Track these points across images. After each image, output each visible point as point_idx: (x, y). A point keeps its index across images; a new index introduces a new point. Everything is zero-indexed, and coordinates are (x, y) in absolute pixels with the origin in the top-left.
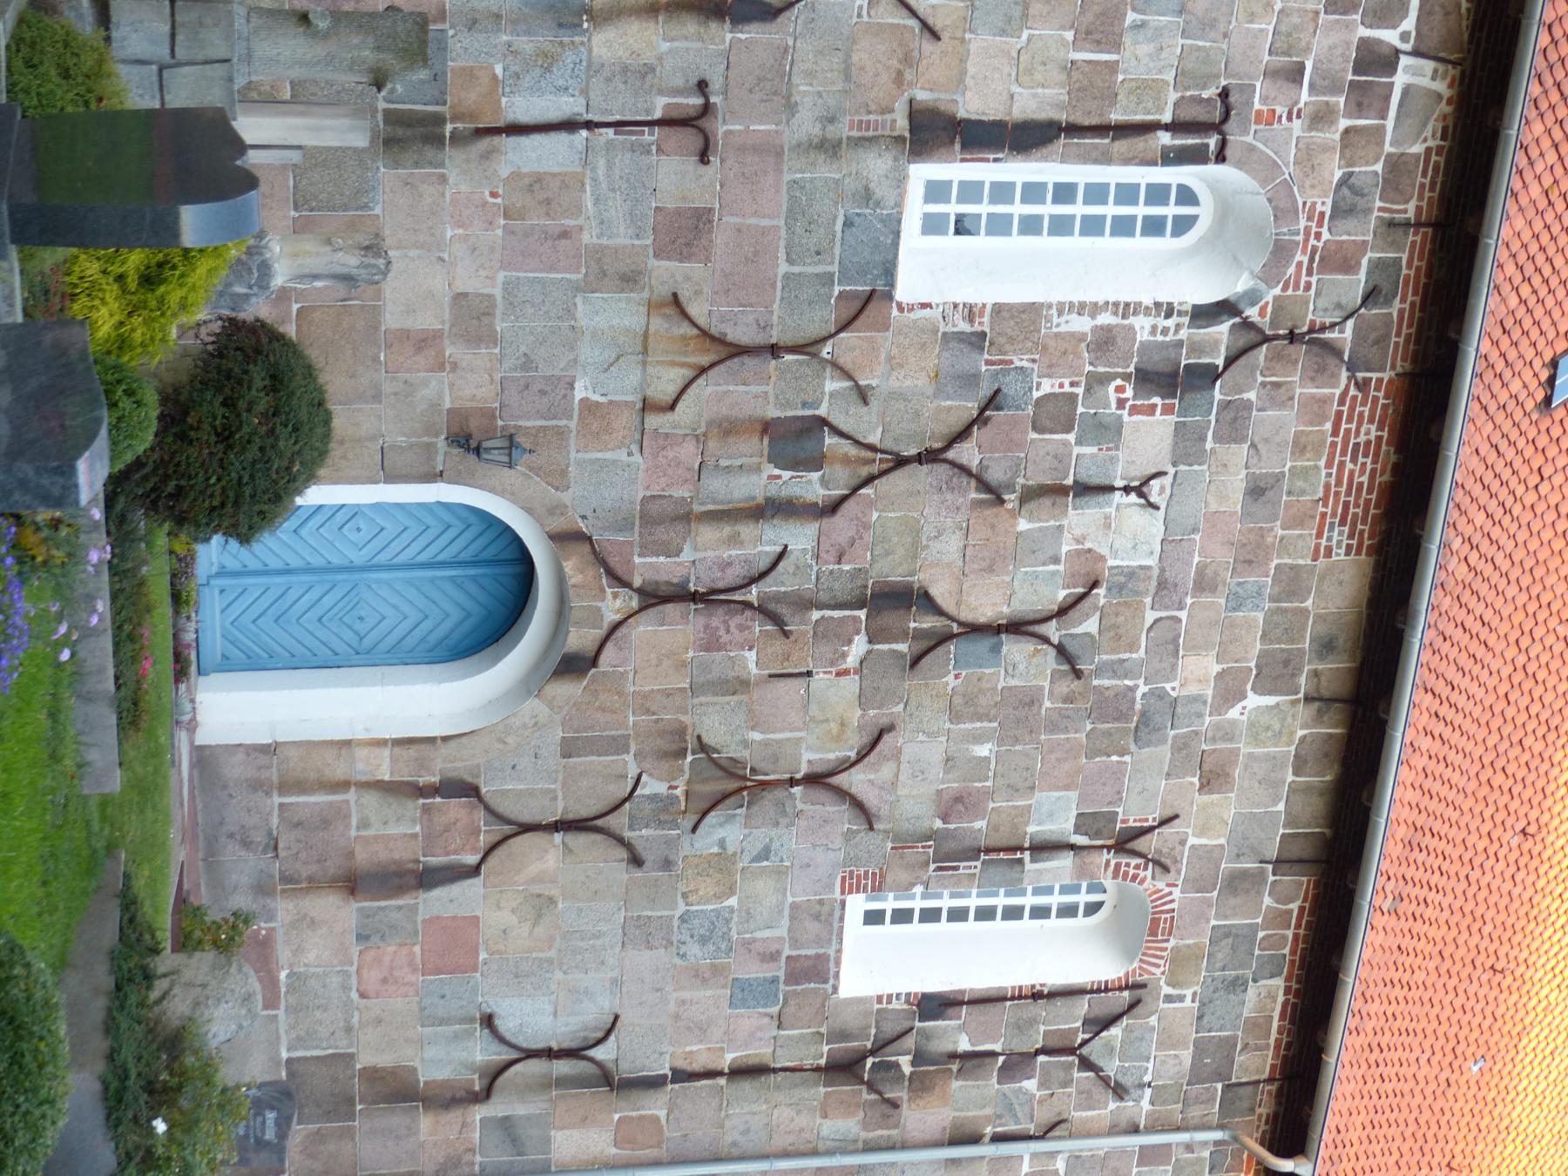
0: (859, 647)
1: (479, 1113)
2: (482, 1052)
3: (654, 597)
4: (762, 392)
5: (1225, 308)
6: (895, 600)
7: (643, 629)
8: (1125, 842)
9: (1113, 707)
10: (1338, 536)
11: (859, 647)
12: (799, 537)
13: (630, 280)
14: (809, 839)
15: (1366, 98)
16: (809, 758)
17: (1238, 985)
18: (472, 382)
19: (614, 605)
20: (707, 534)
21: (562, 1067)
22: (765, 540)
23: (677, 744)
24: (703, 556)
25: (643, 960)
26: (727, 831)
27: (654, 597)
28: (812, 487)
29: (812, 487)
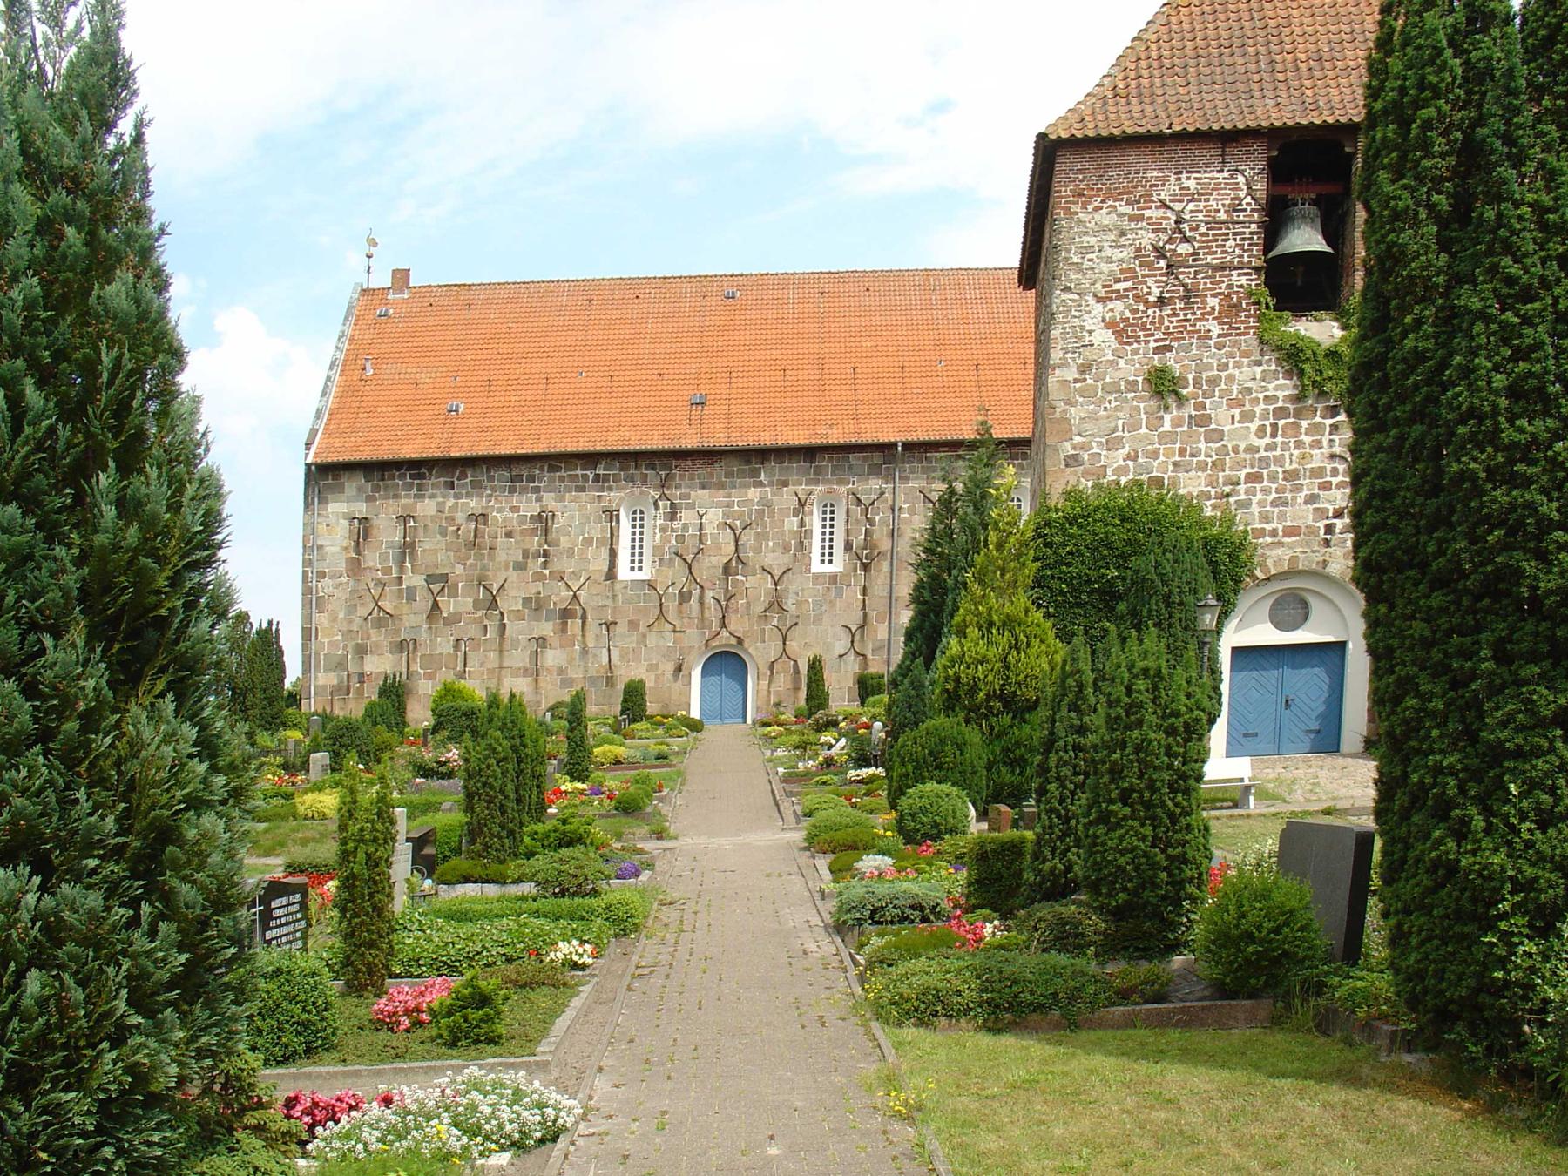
0: (739, 577)
1: (870, 656)
2: (852, 656)
3: (723, 625)
4: (671, 606)
5: (656, 503)
6: (727, 570)
7: (732, 628)
8: (802, 504)
9: (760, 513)
10: (716, 465)
11: (739, 577)
12: (709, 594)
13: (644, 636)
14: (794, 586)
15: (606, 479)
16: (770, 585)
17: (850, 467)
18: (669, 668)
19: (725, 633)
20: (707, 615)
21: (857, 638)
22: (709, 601)
23: (764, 617)
24: (713, 613)
25: (826, 620)
26: (789, 604)
27: (723, 625)
28: (696, 592)
29: (696, 592)
